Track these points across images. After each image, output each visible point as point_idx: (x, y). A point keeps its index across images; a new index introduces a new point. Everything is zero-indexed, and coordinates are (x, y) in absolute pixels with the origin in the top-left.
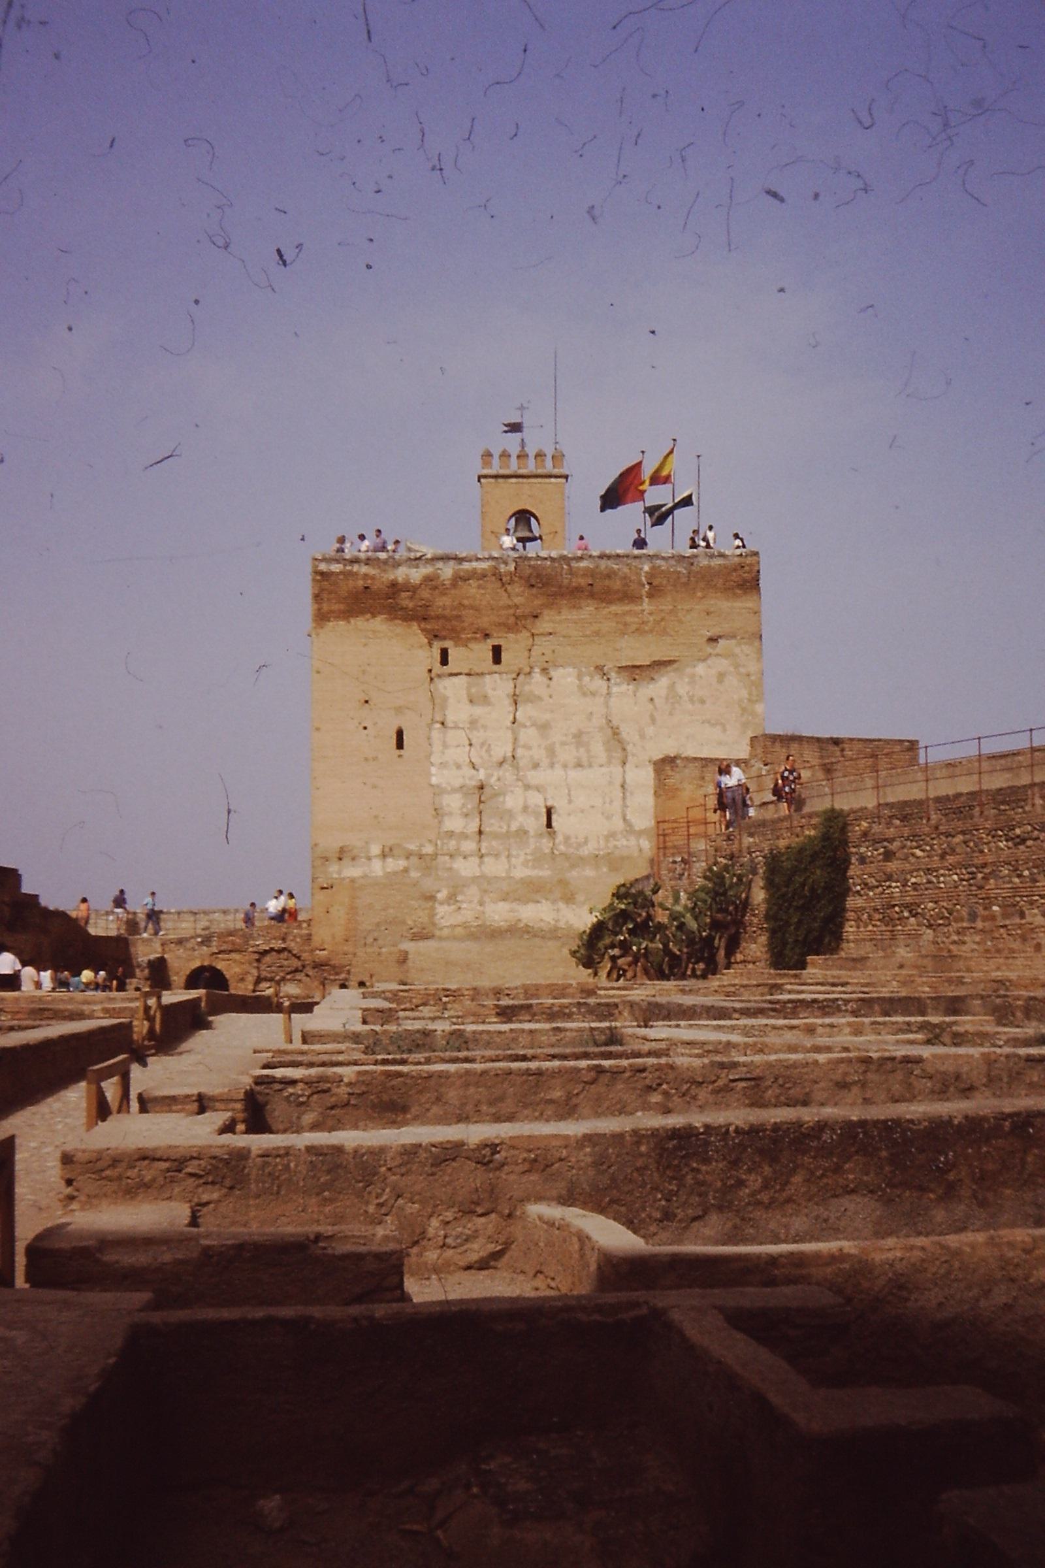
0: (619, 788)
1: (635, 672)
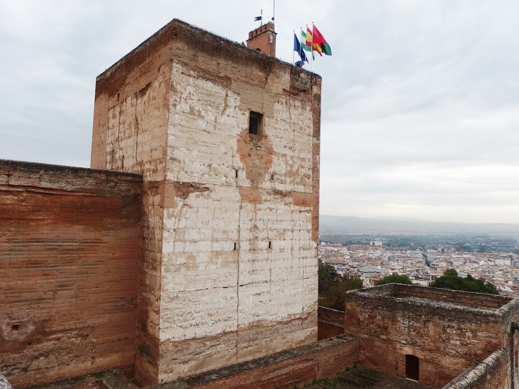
1: (143, 92)
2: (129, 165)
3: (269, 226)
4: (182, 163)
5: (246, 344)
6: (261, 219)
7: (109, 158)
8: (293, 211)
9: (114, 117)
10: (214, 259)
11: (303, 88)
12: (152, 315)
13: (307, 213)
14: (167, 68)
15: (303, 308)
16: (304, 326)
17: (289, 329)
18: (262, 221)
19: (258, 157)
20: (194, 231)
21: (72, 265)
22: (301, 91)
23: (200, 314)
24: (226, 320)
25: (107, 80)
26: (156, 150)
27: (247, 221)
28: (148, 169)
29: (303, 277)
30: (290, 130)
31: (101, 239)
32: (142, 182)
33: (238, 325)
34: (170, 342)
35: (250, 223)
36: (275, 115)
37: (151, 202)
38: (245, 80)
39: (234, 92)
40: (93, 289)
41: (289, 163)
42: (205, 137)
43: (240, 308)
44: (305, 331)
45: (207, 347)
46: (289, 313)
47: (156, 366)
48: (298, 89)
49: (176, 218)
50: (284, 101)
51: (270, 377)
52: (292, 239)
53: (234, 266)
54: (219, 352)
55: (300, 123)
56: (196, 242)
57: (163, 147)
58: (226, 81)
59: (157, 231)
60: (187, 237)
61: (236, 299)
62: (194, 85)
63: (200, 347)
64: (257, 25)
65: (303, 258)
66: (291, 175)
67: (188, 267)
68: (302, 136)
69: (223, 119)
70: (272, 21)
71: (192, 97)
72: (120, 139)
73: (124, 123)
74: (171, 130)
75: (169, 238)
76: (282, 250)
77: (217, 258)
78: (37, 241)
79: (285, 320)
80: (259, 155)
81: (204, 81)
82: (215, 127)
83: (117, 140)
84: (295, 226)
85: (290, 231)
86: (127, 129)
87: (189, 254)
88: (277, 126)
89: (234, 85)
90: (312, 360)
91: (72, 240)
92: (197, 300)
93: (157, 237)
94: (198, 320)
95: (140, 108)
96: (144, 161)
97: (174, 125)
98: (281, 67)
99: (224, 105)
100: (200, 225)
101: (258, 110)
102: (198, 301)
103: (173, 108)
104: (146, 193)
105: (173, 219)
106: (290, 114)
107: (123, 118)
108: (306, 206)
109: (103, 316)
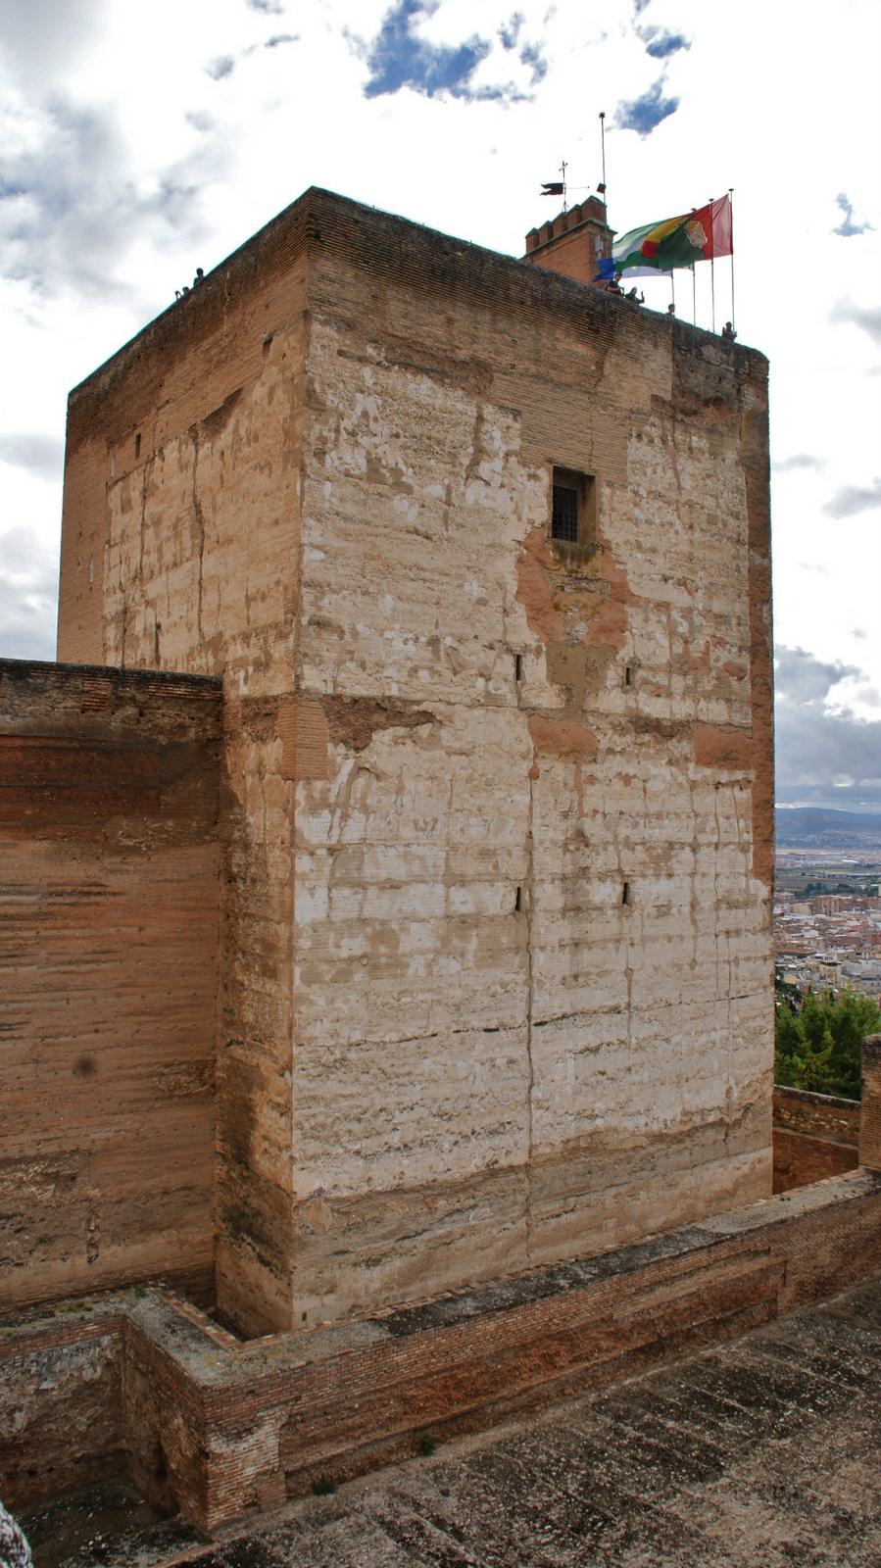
0: (197, 587)
1: (216, 420)
2: (177, 654)
3: (624, 831)
4: (348, 637)
5: (555, 1206)
6: (596, 812)
7: (112, 633)
8: (693, 785)
9: (126, 507)
10: (456, 942)
11: (711, 394)
12: (267, 1119)
13: (736, 789)
14: (293, 340)
15: (729, 1092)
16: (732, 1145)
17: (685, 1158)
18: (599, 816)
19: (584, 612)
20: (392, 852)
21: (21, 965)
22: (706, 403)
23: (414, 1115)
24: (493, 1133)
25: (103, 398)
26: (264, 598)
27: (554, 817)
28: (241, 658)
29: (727, 993)
30: (678, 527)
31: (99, 882)
32: (221, 701)
33: (532, 1147)
34: (326, 1200)
35: (563, 826)
36: (632, 479)
37: (251, 762)
38: (533, 369)
39: (501, 407)
40: (85, 1037)
41: (681, 630)
42: (417, 553)
43: (537, 1093)
44: (735, 1162)
45: (439, 1215)
46: (688, 1109)
47: (283, 1271)
48: (698, 396)
49: (333, 813)
50: (655, 432)
51: (640, 1307)
52: (693, 874)
53: (517, 960)
54: (473, 1230)
55: (710, 502)
56: (398, 887)
57: (286, 588)
58: (472, 375)
59: (275, 855)
60: (369, 871)
61: (524, 1065)
62: (379, 389)
63: (418, 1215)
64: (551, 209)
65: (727, 933)
66: (685, 668)
67: (376, 967)
68: (716, 544)
69: (473, 493)
70: (599, 196)
71: (372, 425)
72: (146, 572)
73: (157, 523)
74: (313, 533)
75: (312, 876)
76: (664, 910)
77: (465, 938)
79: (674, 1130)
80: (585, 606)
81: (409, 376)
82: (446, 518)
83: (138, 577)
84: (702, 831)
85: (688, 849)
86: (168, 539)
87: (378, 927)
88: (637, 512)
89: (500, 386)
90: (768, 1252)
92: (405, 1070)
93: (277, 872)
94: (409, 1133)
95: (207, 472)
96: (227, 636)
97: (319, 517)
98: (642, 328)
99: (471, 450)
100: (407, 833)
101: (574, 462)
102: (409, 1073)
103: (315, 460)
104: (235, 735)
105: (326, 813)
106: (677, 474)
107: (152, 507)
108: (736, 767)
109: (117, 1118)
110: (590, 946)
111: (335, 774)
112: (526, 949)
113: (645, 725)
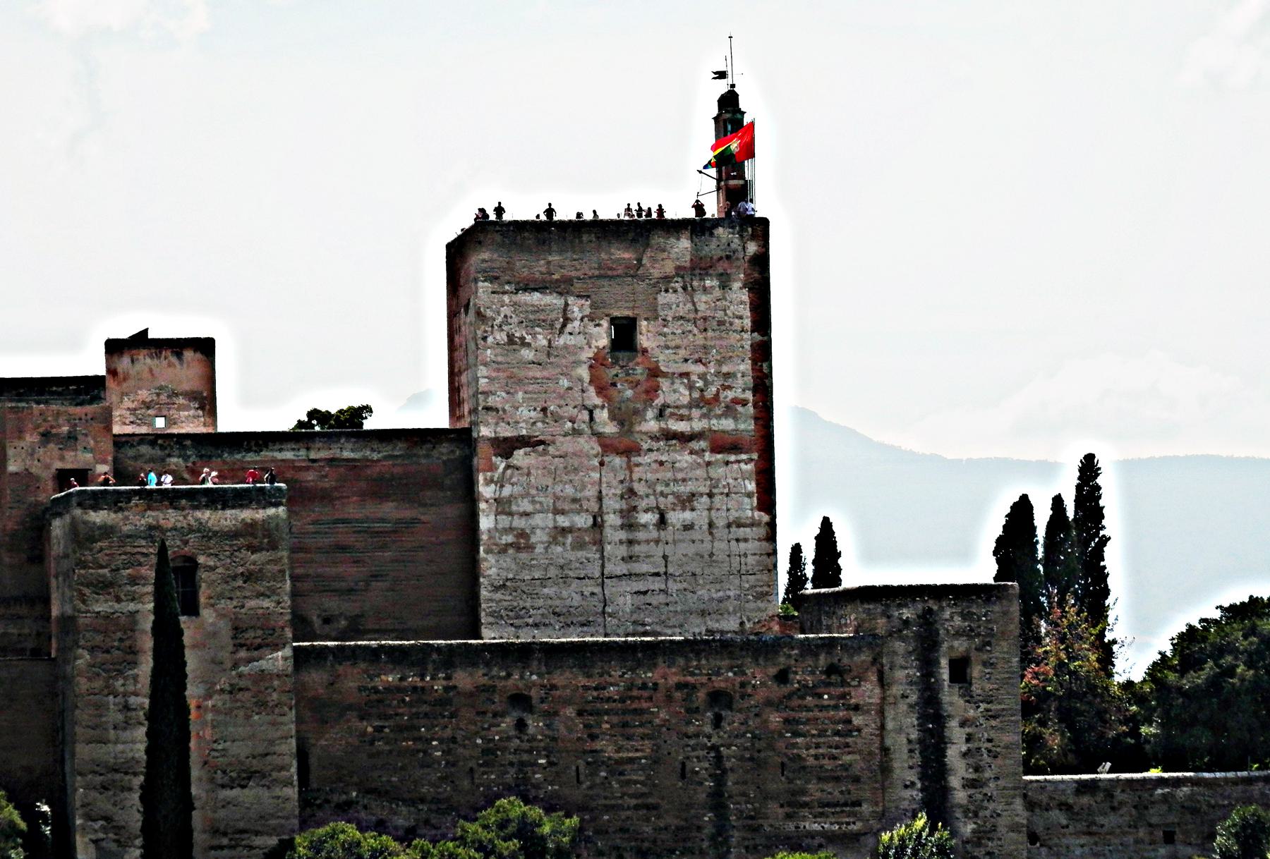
3: (659, 488)
8: (709, 464)
15: (742, 624)
27: (615, 483)
30: (696, 331)
42: (537, 372)
43: (609, 610)
52: (709, 509)
58: (562, 287)
60: (514, 508)
69: (561, 341)
76: (688, 527)
78: (344, 521)
82: (549, 355)
89: (578, 286)
91: (383, 520)
97: (485, 364)
100: (533, 492)
105: (493, 486)
106: (694, 304)
110: (639, 543)
111: (497, 469)
112: (600, 543)
113: (669, 436)
